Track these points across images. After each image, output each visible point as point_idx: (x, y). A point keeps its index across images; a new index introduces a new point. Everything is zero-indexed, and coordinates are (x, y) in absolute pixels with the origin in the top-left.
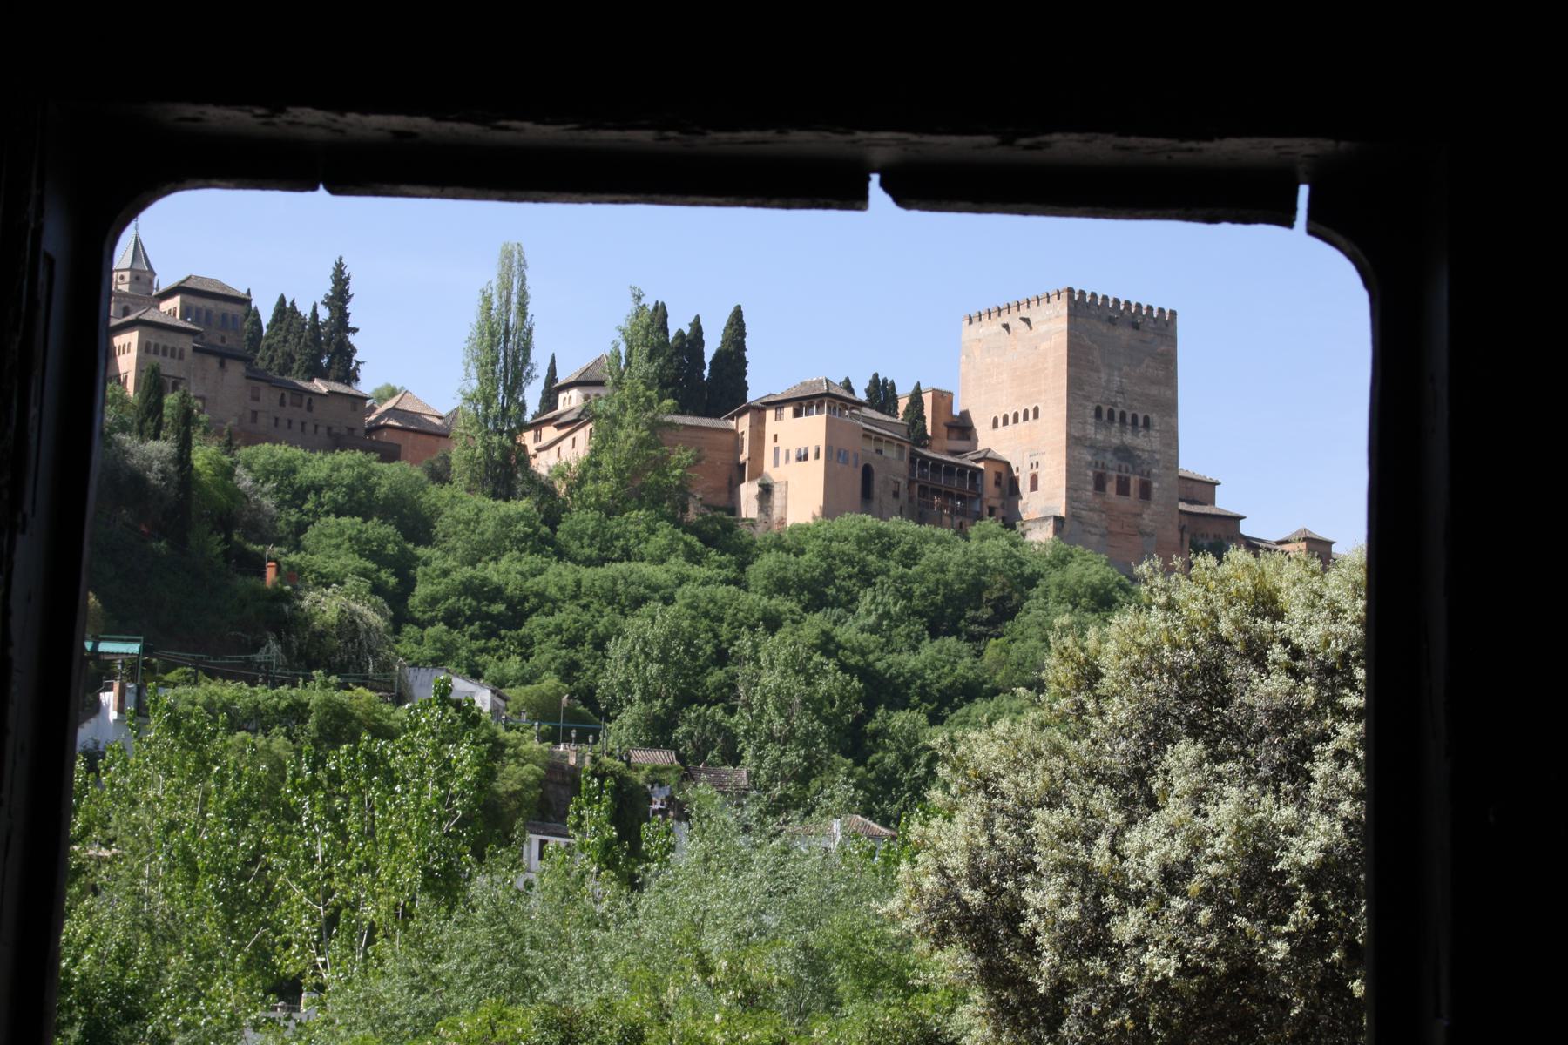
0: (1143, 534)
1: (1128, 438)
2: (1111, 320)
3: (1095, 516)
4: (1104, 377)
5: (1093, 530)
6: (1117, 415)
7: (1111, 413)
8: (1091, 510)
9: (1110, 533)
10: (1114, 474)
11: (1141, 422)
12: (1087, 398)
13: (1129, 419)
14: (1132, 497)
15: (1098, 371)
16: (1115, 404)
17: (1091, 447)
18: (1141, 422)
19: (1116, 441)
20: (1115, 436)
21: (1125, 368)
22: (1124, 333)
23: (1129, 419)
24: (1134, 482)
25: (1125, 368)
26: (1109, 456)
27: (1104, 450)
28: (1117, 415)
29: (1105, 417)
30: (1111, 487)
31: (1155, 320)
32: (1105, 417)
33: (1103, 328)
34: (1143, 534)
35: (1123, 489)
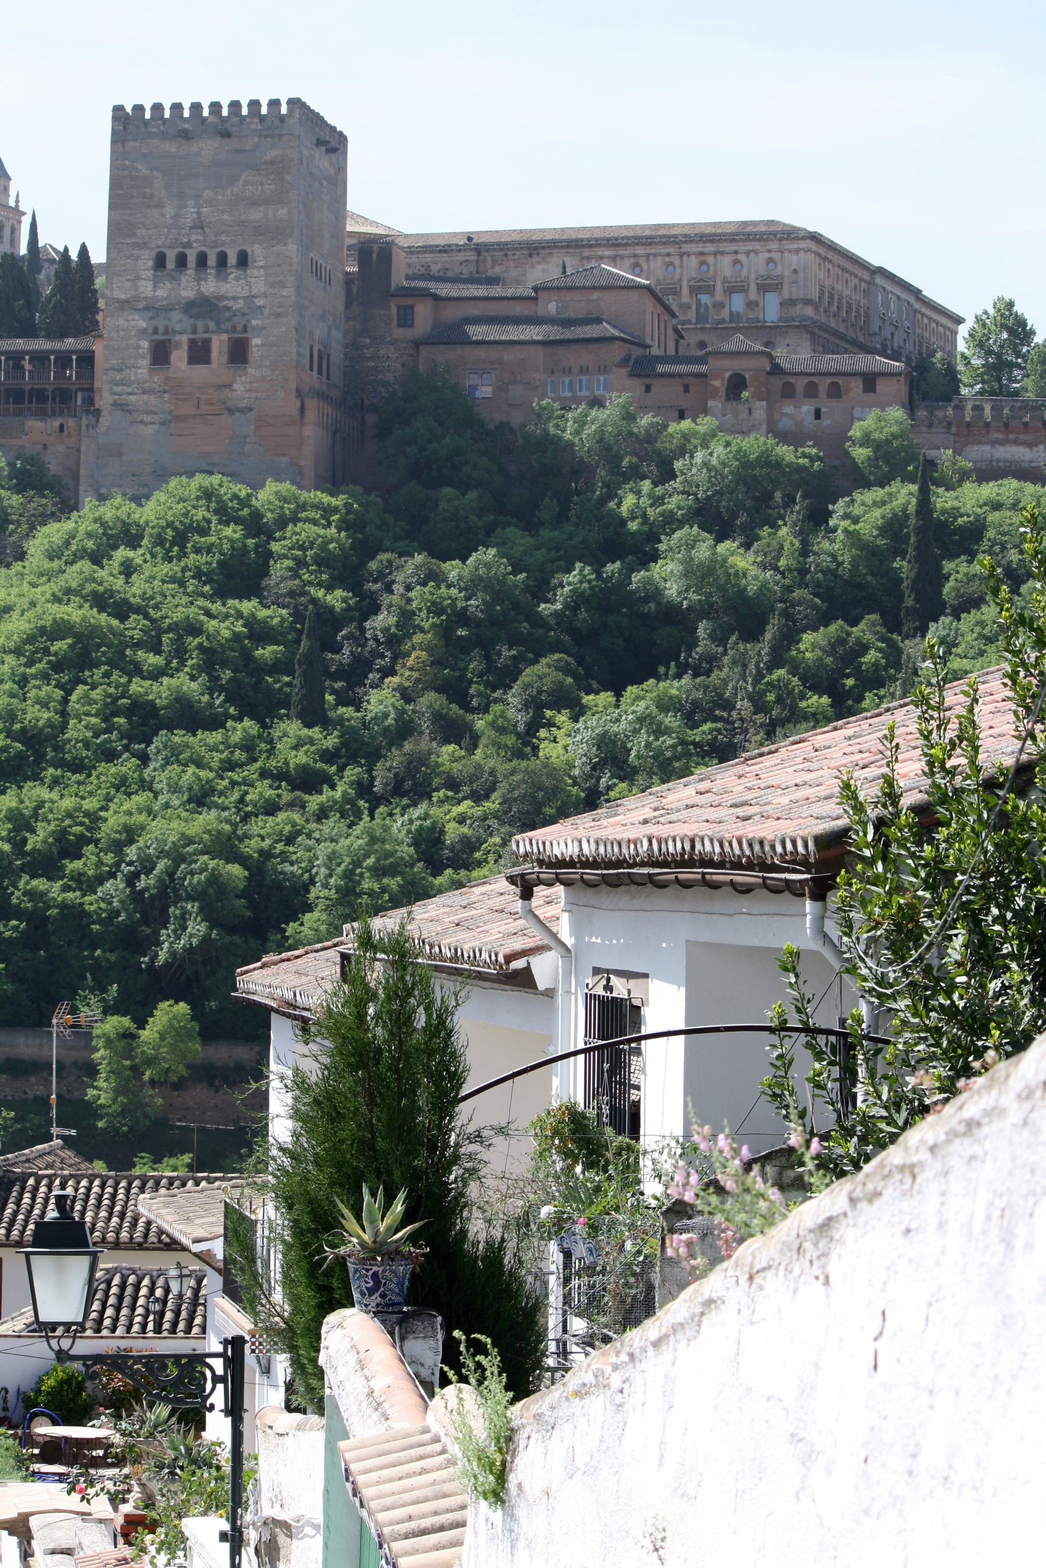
0: (231, 411)
1: (210, 286)
2: (186, 135)
3: (153, 400)
4: (169, 211)
5: (147, 418)
6: (192, 260)
7: (182, 261)
8: (145, 392)
9: (177, 417)
10: (184, 338)
11: (232, 260)
12: (138, 246)
13: (212, 261)
14: (215, 364)
15: (159, 205)
16: (189, 245)
17: (147, 308)
18: (232, 260)
19: (188, 293)
20: (187, 287)
21: (207, 194)
22: (207, 148)
23: (212, 261)
24: (219, 344)
25: (207, 194)
26: (176, 316)
27: (168, 309)
28: (192, 260)
29: (171, 264)
30: (179, 358)
31: (262, 119)
32: (171, 264)
33: (172, 147)
34: (231, 411)
35: (199, 353)
